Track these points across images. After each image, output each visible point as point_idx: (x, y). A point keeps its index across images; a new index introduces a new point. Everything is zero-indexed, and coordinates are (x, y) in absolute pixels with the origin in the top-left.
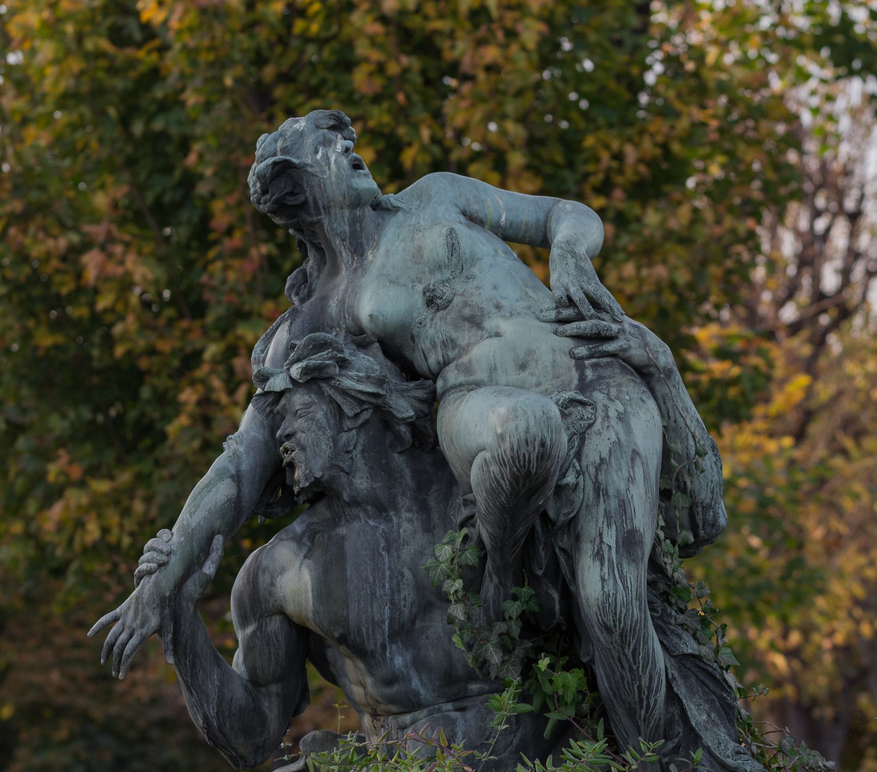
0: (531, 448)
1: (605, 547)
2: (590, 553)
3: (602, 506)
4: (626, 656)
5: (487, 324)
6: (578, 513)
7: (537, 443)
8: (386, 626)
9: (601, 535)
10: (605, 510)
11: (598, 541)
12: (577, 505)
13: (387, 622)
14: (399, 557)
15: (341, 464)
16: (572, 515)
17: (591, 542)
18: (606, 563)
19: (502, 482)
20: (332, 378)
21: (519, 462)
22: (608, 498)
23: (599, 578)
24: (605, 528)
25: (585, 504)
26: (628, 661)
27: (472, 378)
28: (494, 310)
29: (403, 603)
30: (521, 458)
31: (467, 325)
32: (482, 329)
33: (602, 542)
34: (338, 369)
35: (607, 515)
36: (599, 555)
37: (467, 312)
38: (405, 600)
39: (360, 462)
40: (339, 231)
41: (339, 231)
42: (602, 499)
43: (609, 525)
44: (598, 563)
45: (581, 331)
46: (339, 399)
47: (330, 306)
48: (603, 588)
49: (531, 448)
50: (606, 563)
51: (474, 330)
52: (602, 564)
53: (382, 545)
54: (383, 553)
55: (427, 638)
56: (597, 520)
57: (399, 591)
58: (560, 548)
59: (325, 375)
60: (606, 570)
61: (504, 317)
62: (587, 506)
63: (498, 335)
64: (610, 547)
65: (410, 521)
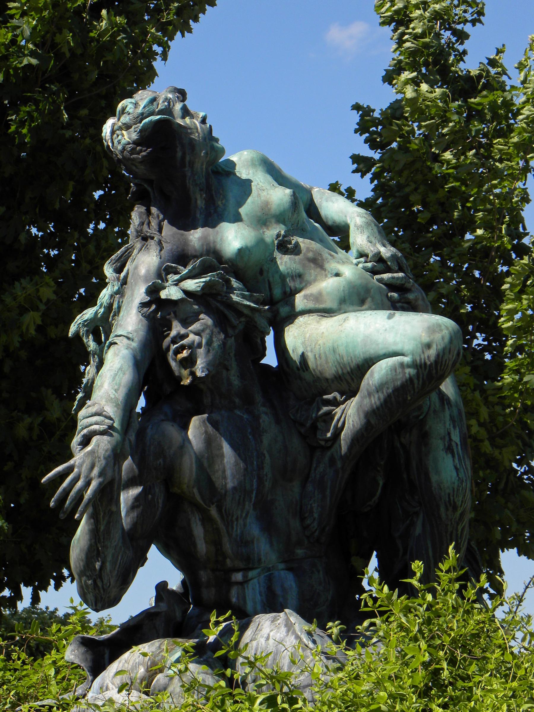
0: (451, 356)
1: (453, 444)
2: (441, 447)
3: (447, 413)
4: (457, 531)
5: (327, 266)
6: (425, 417)
7: (456, 352)
8: (254, 495)
9: (449, 434)
10: (450, 415)
11: (447, 438)
12: (425, 409)
13: (254, 492)
14: (262, 442)
15: (226, 362)
16: (421, 417)
17: (441, 439)
18: (456, 456)
19: (416, 381)
20: (218, 294)
21: (441, 367)
22: (451, 406)
23: (453, 467)
24: (452, 429)
25: (432, 409)
26: (457, 535)
27: (322, 306)
28: (329, 257)
29: (265, 478)
30: (444, 363)
31: (312, 265)
32: (325, 270)
33: (450, 440)
34: (225, 287)
35: (452, 418)
36: (449, 449)
37: (310, 255)
38: (267, 476)
39: (234, 364)
40: (199, 182)
41: (199, 182)
42: (446, 407)
43: (454, 427)
44: (450, 455)
45: (394, 281)
46: (226, 312)
47: (191, 241)
48: (458, 475)
49: (451, 356)
50: (456, 456)
51: (318, 270)
52: (453, 456)
53: (249, 430)
54: (250, 437)
55: (276, 509)
56: (445, 423)
57: (263, 468)
58: (401, 444)
59: (214, 291)
60: (457, 461)
61: (338, 262)
62: (435, 411)
63: (337, 275)
64: (457, 444)
65: (266, 414)
